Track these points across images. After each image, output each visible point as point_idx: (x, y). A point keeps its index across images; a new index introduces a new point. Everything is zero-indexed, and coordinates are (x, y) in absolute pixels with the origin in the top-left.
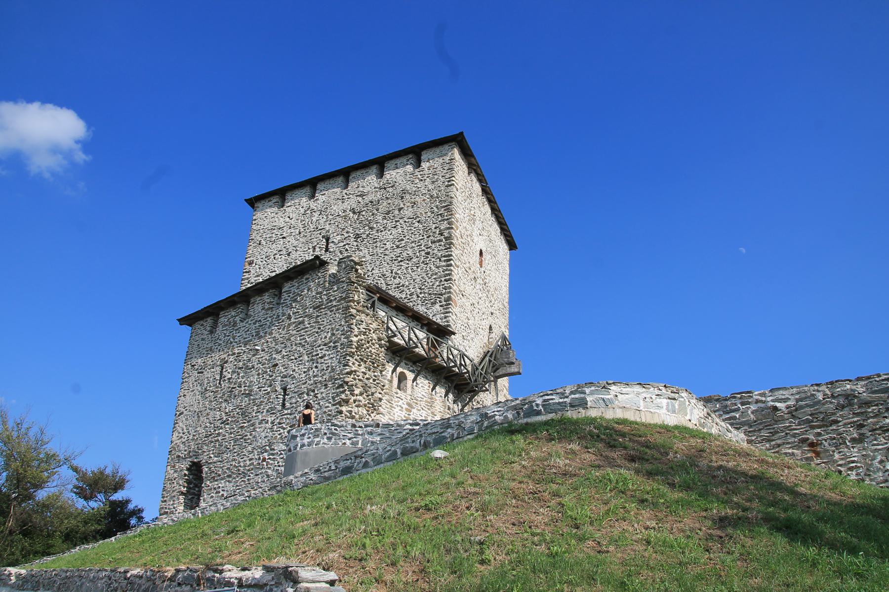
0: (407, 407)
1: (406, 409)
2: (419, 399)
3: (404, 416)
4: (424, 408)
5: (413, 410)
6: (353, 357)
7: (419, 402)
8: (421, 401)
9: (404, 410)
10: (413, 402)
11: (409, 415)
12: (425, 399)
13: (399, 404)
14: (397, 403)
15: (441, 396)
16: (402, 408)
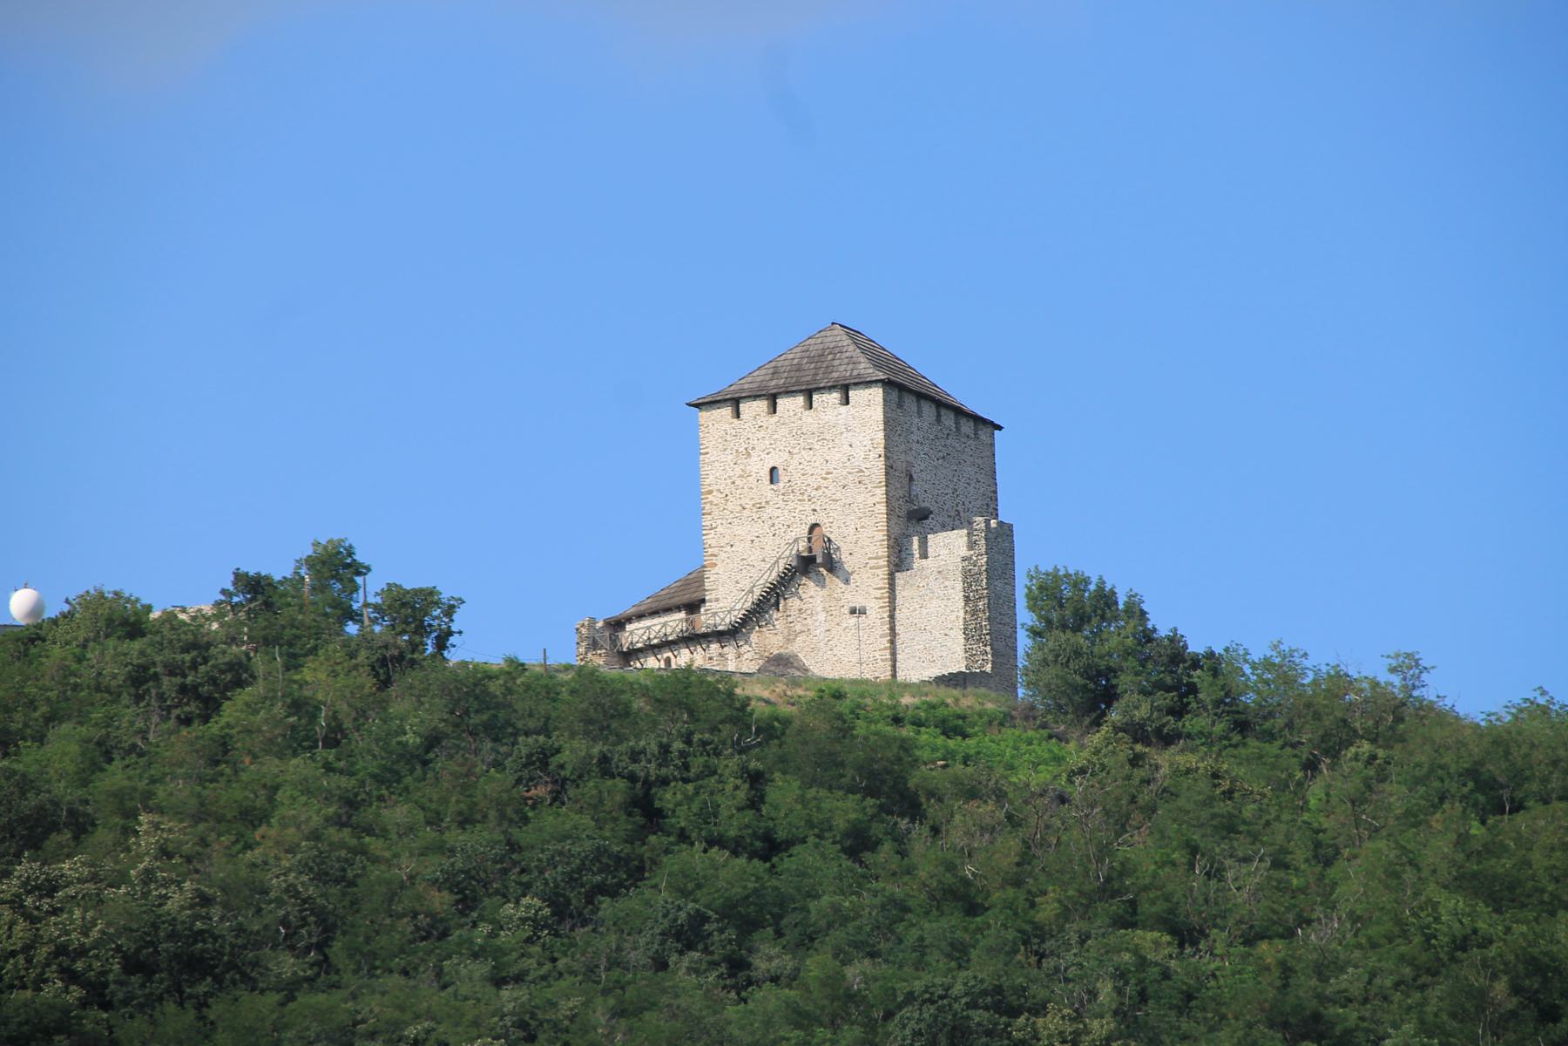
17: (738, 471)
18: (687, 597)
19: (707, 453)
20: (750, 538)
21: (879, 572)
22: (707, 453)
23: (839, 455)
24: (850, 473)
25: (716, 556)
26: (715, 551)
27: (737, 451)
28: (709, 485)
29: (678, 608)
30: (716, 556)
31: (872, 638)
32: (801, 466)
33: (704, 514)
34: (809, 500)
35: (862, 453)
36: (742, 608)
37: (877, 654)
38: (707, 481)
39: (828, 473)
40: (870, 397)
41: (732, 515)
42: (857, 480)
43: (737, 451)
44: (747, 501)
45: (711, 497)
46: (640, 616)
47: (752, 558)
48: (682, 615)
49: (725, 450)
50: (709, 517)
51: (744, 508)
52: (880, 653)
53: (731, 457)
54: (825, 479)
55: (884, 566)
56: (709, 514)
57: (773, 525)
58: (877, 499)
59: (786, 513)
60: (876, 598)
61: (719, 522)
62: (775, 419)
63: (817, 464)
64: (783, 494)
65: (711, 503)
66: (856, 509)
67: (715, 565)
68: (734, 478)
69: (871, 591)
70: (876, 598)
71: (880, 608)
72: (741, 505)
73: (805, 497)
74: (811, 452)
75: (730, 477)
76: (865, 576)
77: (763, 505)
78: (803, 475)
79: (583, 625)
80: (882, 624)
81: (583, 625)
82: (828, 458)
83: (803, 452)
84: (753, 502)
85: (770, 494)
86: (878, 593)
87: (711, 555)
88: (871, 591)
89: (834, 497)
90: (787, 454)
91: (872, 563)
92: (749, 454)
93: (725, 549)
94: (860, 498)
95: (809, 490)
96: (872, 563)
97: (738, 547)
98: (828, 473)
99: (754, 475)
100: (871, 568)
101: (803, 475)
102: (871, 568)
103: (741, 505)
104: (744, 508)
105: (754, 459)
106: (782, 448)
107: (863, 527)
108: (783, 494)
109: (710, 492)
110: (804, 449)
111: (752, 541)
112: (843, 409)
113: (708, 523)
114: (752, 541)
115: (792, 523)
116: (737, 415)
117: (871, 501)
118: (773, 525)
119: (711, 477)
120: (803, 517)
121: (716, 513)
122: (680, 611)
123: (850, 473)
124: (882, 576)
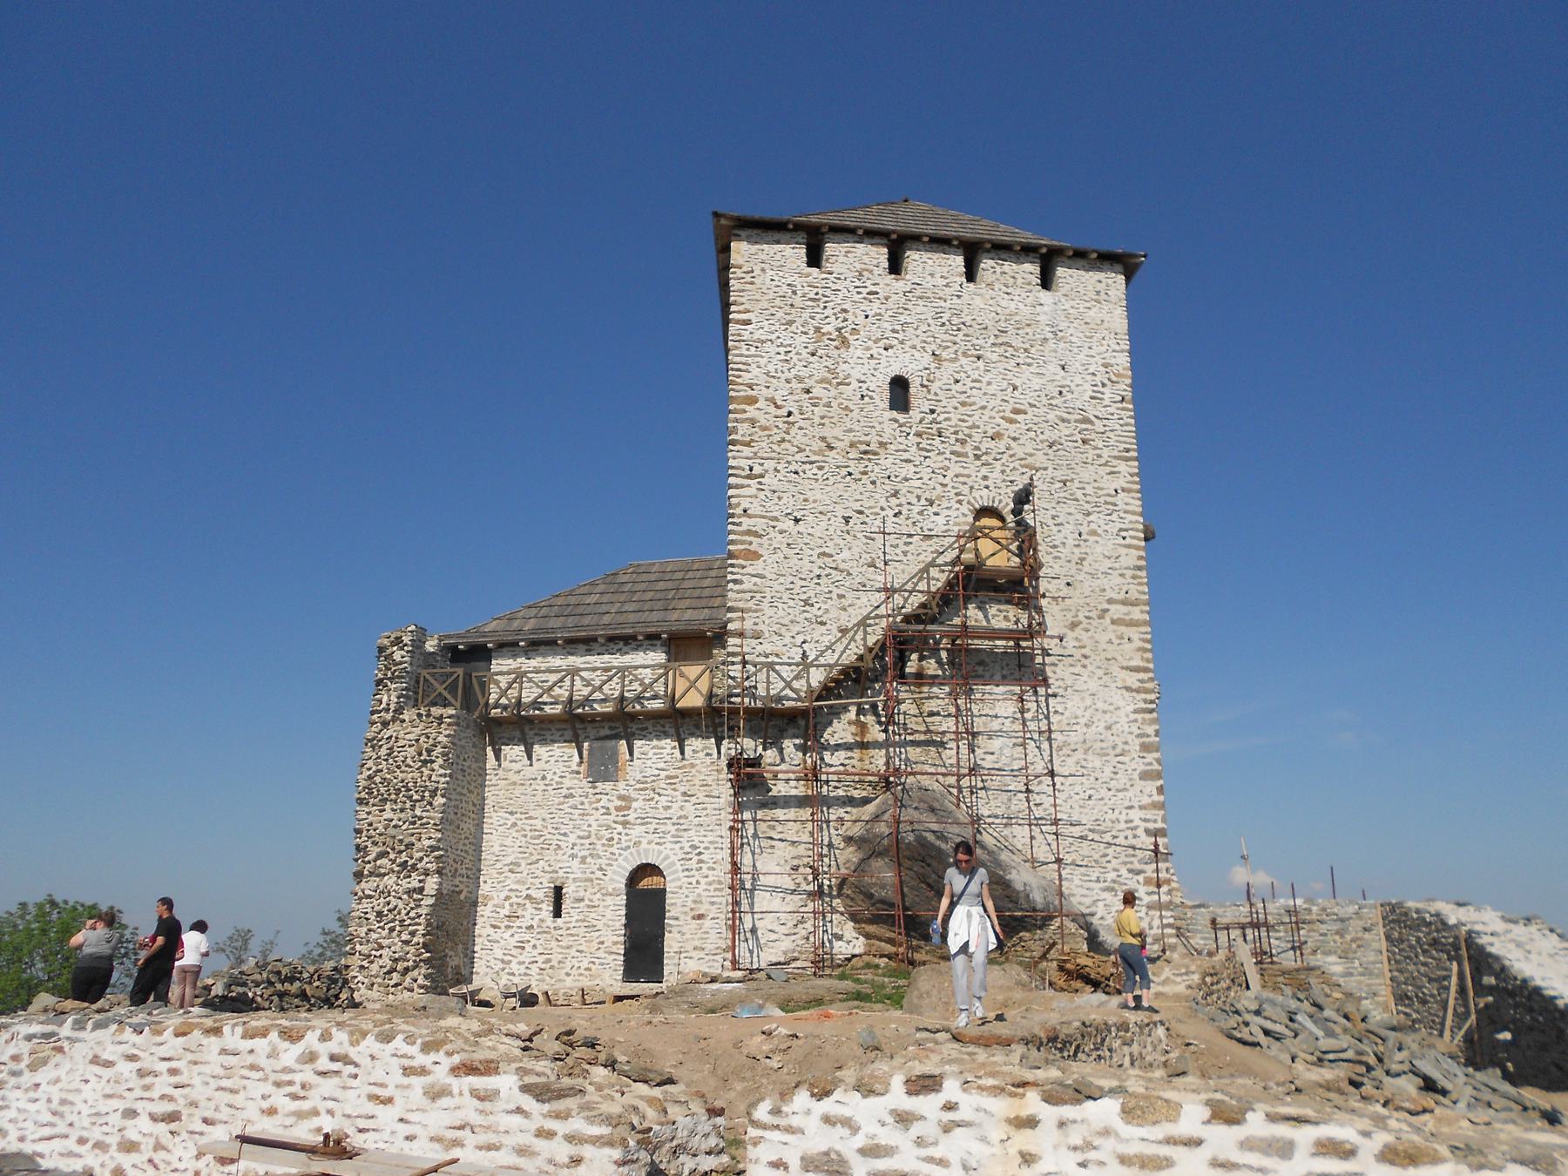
0: (619, 803)
1: (618, 809)
2: (649, 780)
3: (615, 822)
4: (661, 792)
5: (634, 805)
6: (367, 804)
7: (648, 785)
8: (654, 781)
9: (612, 810)
10: (635, 789)
11: (624, 816)
12: (663, 774)
13: (602, 803)
14: (594, 806)
15: (708, 754)
16: (608, 808)
17: (818, 368)
18: (685, 616)
19: (748, 322)
20: (840, 512)
21: (1133, 632)
22: (748, 322)
23: (1037, 383)
24: (1063, 420)
25: (756, 534)
26: (759, 525)
27: (818, 330)
28: (750, 386)
29: (652, 639)
30: (756, 534)
31: (1122, 780)
32: (958, 387)
33: (733, 443)
34: (977, 457)
35: (1087, 386)
36: (836, 664)
37: (1136, 815)
38: (746, 377)
39: (1017, 412)
40: (1100, 287)
41: (798, 457)
42: (1078, 437)
43: (818, 330)
44: (838, 432)
45: (751, 412)
46: (538, 645)
47: (846, 554)
48: (658, 657)
49: (790, 323)
50: (747, 451)
51: (831, 448)
52: (1142, 814)
53: (804, 338)
54: (1011, 421)
55: (1145, 623)
56: (748, 444)
57: (895, 494)
58: (1120, 483)
59: (925, 473)
60: (1128, 689)
61: (770, 465)
62: (899, 285)
63: (992, 389)
64: (919, 435)
65: (753, 422)
66: (1079, 494)
67: (756, 556)
68: (809, 383)
69: (1115, 670)
70: (1128, 689)
71: (1136, 711)
72: (823, 439)
73: (968, 449)
74: (980, 363)
75: (800, 380)
76: (1103, 638)
77: (874, 447)
78: (963, 404)
79: (398, 641)
80: (1146, 748)
81: (398, 641)
82: (1017, 382)
83: (964, 361)
84: (851, 437)
85: (889, 430)
86: (1132, 680)
87: (749, 532)
88: (1115, 670)
89: (1030, 460)
90: (927, 359)
91: (1117, 611)
92: (845, 342)
93: (780, 526)
94: (1086, 474)
95: (977, 437)
96: (1117, 611)
97: (815, 527)
98: (1017, 412)
99: (855, 385)
100: (1113, 622)
101: (963, 404)
102: (1113, 622)
103: (823, 439)
104: (831, 448)
105: (856, 351)
106: (916, 342)
107: (1094, 533)
108: (919, 435)
109: (752, 401)
110: (965, 354)
111: (847, 520)
112: (1044, 296)
113: (744, 463)
114: (847, 520)
115: (940, 498)
116: (814, 259)
117: (1111, 484)
118: (895, 494)
119: (755, 371)
120: (965, 489)
121: (763, 446)
122: (652, 648)
123: (1063, 420)
124: (1138, 644)
